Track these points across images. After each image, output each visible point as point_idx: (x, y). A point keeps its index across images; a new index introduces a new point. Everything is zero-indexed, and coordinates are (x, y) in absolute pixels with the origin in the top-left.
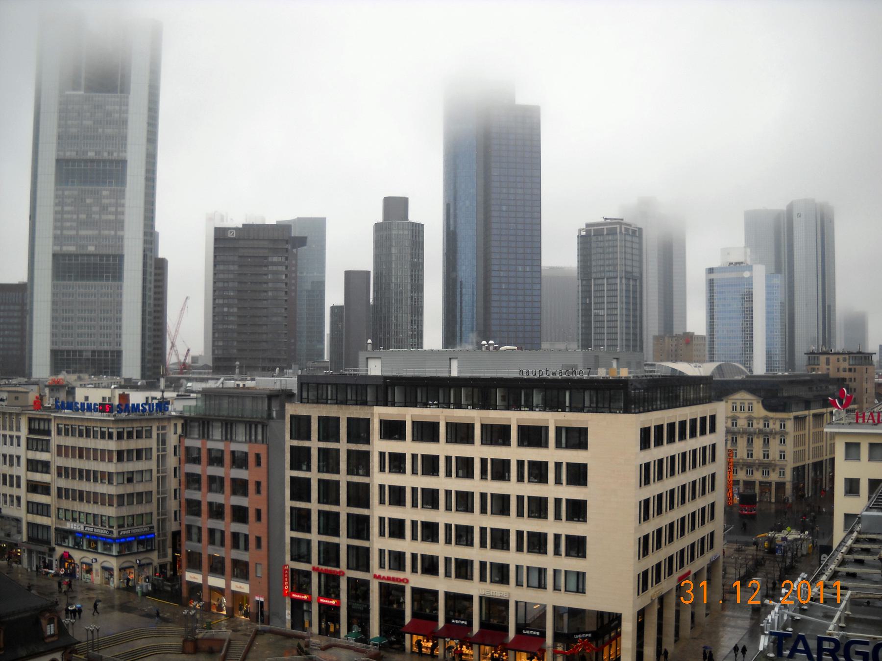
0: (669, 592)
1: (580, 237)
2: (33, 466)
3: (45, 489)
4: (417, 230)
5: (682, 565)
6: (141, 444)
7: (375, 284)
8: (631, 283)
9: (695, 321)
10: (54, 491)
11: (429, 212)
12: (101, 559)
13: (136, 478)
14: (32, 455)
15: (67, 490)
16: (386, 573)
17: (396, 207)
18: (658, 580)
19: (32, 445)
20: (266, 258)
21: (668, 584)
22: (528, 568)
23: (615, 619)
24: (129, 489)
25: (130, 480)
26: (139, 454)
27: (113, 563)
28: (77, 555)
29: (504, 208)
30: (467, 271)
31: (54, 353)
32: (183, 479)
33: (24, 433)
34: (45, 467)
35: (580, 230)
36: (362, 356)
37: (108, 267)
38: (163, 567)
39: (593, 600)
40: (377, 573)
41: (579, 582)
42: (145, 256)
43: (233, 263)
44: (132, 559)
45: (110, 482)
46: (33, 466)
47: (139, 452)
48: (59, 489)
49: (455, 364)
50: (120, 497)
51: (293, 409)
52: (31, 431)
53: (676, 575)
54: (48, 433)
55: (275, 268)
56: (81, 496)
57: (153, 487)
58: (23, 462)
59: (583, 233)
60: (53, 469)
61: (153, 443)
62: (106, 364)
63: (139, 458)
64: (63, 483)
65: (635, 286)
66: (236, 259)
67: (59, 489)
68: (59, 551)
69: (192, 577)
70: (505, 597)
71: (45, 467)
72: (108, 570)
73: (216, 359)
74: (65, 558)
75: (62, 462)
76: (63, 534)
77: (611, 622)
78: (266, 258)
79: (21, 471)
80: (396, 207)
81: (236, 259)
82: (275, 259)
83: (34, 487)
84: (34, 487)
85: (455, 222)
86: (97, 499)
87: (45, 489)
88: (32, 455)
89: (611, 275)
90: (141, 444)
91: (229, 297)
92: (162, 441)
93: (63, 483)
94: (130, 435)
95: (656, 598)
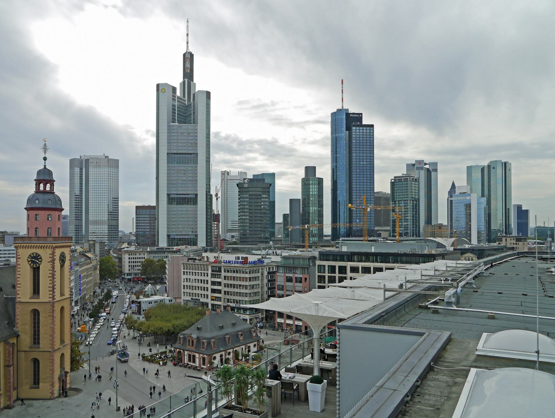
1: (392, 183)
2: (213, 283)
3: (219, 291)
4: (320, 181)
7: (302, 204)
8: (415, 202)
9: (442, 217)
10: (223, 292)
11: (324, 172)
14: (213, 280)
15: (228, 292)
17: (310, 171)
19: (213, 276)
20: (260, 195)
24: (253, 291)
25: (253, 288)
29: (358, 171)
34: (219, 284)
35: (392, 179)
37: (194, 200)
42: (207, 194)
43: (247, 198)
45: (246, 288)
46: (213, 283)
48: (225, 292)
50: (250, 293)
55: (264, 200)
57: (260, 290)
58: (209, 282)
59: (393, 181)
60: (223, 285)
64: (227, 289)
65: (416, 204)
66: (248, 196)
67: (225, 292)
71: (219, 284)
75: (226, 282)
78: (260, 195)
79: (209, 286)
80: (310, 171)
81: (248, 196)
82: (264, 196)
83: (213, 291)
84: (213, 291)
85: (336, 177)
86: (240, 294)
87: (219, 291)
88: (213, 280)
89: (406, 199)
91: (245, 212)
93: (227, 289)
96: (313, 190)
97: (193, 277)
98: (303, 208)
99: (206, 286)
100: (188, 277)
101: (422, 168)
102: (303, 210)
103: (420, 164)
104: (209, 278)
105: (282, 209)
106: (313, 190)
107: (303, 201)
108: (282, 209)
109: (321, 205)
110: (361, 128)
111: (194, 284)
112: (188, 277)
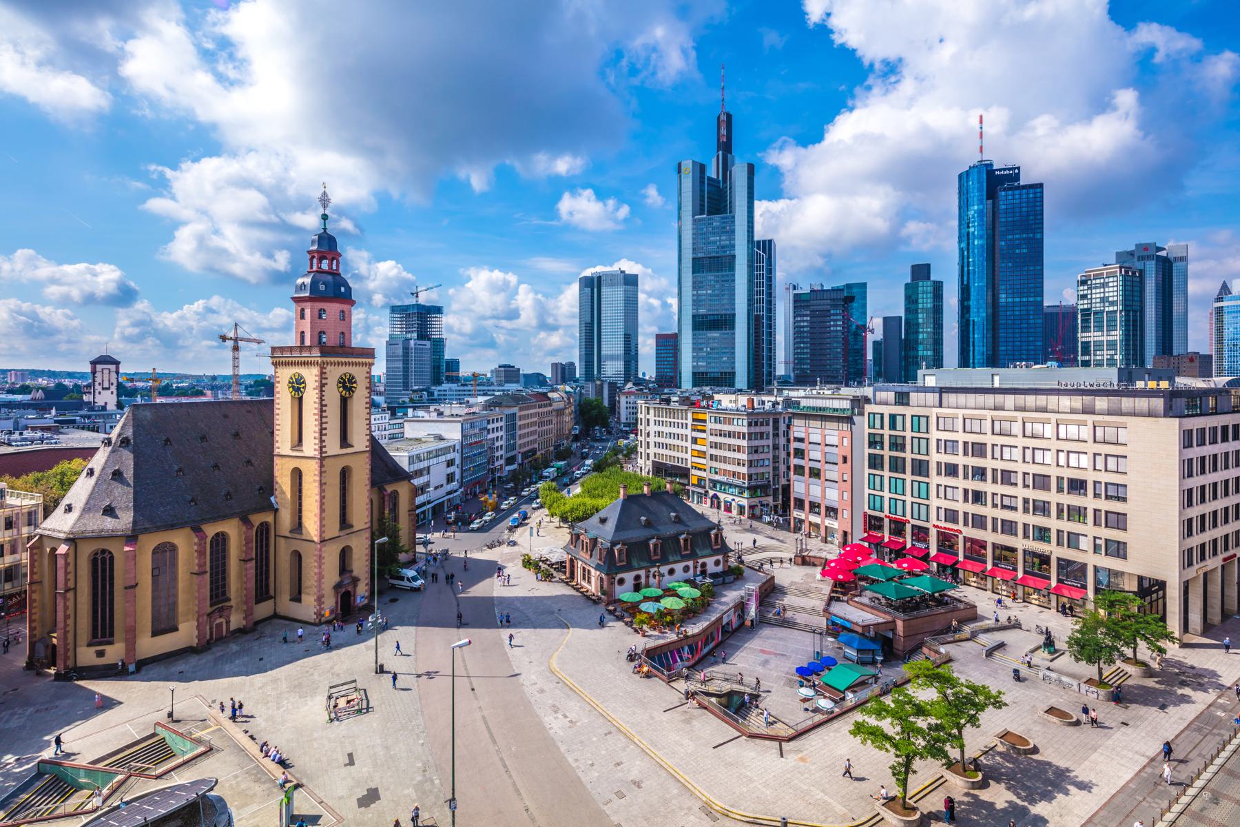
0: (1215, 570)
4: (938, 289)
5: (1226, 549)
6: (763, 429)
11: (948, 276)
12: (737, 499)
13: (760, 450)
16: (943, 524)
17: (921, 272)
18: (1203, 558)
21: (1214, 563)
22: (1069, 533)
23: (1162, 585)
25: (756, 452)
26: (762, 435)
27: (744, 502)
28: (722, 496)
30: (978, 316)
31: (694, 374)
32: (792, 452)
33: (690, 421)
36: (920, 373)
38: (776, 506)
39: (1134, 566)
40: (935, 523)
41: (1118, 549)
44: (757, 500)
47: (762, 434)
49: (997, 379)
51: (869, 408)
52: (694, 420)
53: (1221, 557)
54: (704, 421)
56: (725, 460)
61: (770, 429)
62: (725, 381)
63: (762, 438)
68: (711, 493)
69: (796, 513)
70: (1047, 553)
72: (741, 508)
73: (797, 376)
74: (715, 496)
76: (714, 483)
77: (1151, 586)
79: (688, 444)
80: (921, 272)
90: (763, 429)
92: (776, 428)
93: (714, 452)
94: (756, 424)
95: (1201, 573)
96: (925, 302)
97: (667, 430)
98: (906, 330)
99: (684, 444)
100: (661, 429)
101: (1150, 257)
102: (906, 334)
103: (1146, 249)
104: (688, 432)
105: (876, 331)
106: (925, 302)
107: (906, 323)
108: (876, 331)
109: (938, 326)
110: (1017, 192)
111: (668, 441)
112: (661, 429)
